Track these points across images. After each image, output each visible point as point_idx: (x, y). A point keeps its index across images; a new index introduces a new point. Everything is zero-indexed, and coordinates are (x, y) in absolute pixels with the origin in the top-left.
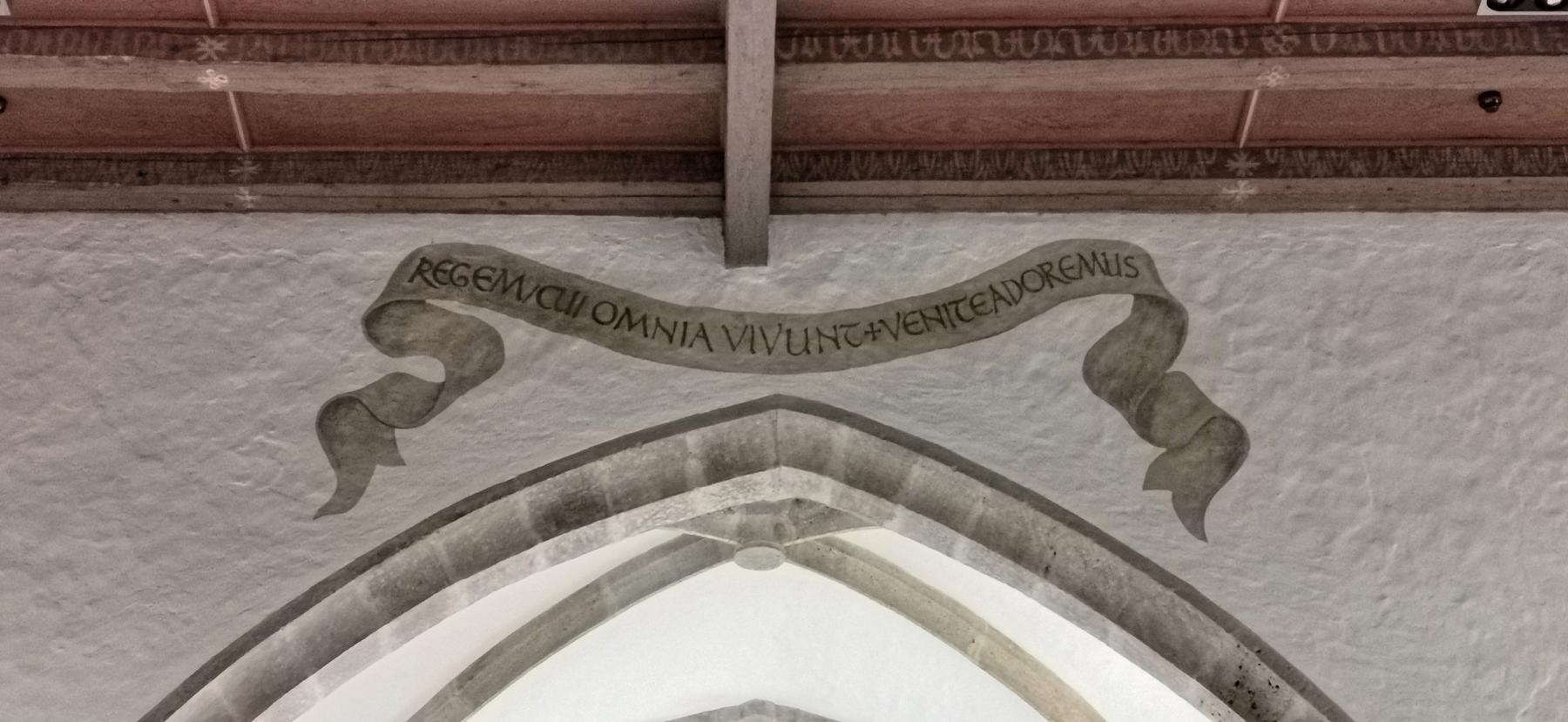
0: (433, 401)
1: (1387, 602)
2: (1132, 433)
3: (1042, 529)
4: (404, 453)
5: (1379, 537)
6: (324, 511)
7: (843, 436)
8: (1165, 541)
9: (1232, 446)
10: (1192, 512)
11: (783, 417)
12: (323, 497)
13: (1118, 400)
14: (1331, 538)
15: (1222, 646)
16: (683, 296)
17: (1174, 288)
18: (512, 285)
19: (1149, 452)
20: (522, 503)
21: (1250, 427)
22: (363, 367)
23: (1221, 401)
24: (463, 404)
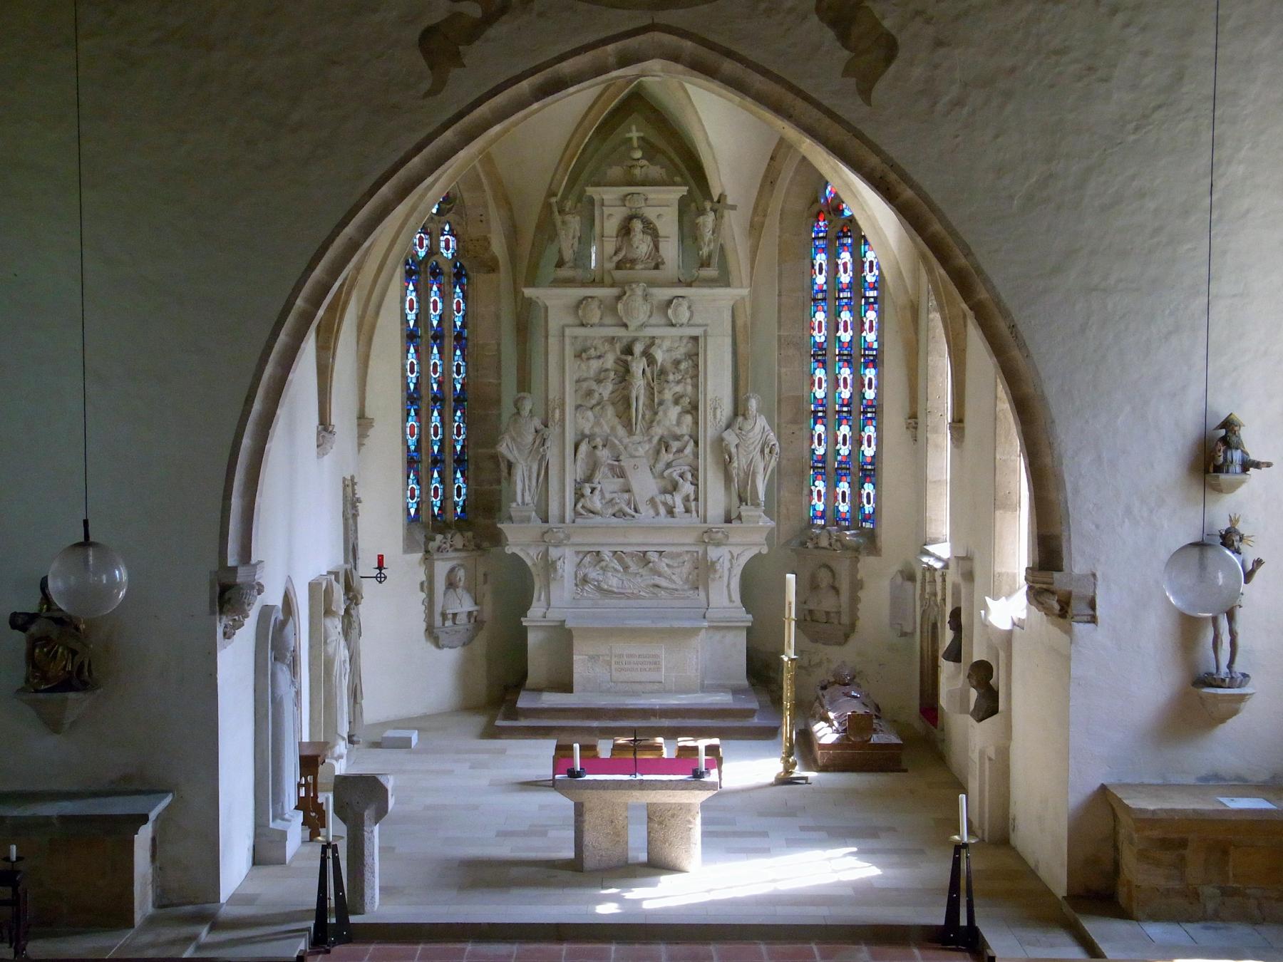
1: (959, 139)
2: (838, 44)
3: (789, 98)
4: (465, 61)
5: (958, 103)
6: (429, 94)
7: (688, 44)
8: (851, 108)
9: (890, 48)
10: (865, 92)
12: (426, 85)
13: (833, 24)
14: (935, 103)
15: (874, 161)
19: (846, 53)
20: (525, 85)
23: (887, 24)
24: (492, 32)
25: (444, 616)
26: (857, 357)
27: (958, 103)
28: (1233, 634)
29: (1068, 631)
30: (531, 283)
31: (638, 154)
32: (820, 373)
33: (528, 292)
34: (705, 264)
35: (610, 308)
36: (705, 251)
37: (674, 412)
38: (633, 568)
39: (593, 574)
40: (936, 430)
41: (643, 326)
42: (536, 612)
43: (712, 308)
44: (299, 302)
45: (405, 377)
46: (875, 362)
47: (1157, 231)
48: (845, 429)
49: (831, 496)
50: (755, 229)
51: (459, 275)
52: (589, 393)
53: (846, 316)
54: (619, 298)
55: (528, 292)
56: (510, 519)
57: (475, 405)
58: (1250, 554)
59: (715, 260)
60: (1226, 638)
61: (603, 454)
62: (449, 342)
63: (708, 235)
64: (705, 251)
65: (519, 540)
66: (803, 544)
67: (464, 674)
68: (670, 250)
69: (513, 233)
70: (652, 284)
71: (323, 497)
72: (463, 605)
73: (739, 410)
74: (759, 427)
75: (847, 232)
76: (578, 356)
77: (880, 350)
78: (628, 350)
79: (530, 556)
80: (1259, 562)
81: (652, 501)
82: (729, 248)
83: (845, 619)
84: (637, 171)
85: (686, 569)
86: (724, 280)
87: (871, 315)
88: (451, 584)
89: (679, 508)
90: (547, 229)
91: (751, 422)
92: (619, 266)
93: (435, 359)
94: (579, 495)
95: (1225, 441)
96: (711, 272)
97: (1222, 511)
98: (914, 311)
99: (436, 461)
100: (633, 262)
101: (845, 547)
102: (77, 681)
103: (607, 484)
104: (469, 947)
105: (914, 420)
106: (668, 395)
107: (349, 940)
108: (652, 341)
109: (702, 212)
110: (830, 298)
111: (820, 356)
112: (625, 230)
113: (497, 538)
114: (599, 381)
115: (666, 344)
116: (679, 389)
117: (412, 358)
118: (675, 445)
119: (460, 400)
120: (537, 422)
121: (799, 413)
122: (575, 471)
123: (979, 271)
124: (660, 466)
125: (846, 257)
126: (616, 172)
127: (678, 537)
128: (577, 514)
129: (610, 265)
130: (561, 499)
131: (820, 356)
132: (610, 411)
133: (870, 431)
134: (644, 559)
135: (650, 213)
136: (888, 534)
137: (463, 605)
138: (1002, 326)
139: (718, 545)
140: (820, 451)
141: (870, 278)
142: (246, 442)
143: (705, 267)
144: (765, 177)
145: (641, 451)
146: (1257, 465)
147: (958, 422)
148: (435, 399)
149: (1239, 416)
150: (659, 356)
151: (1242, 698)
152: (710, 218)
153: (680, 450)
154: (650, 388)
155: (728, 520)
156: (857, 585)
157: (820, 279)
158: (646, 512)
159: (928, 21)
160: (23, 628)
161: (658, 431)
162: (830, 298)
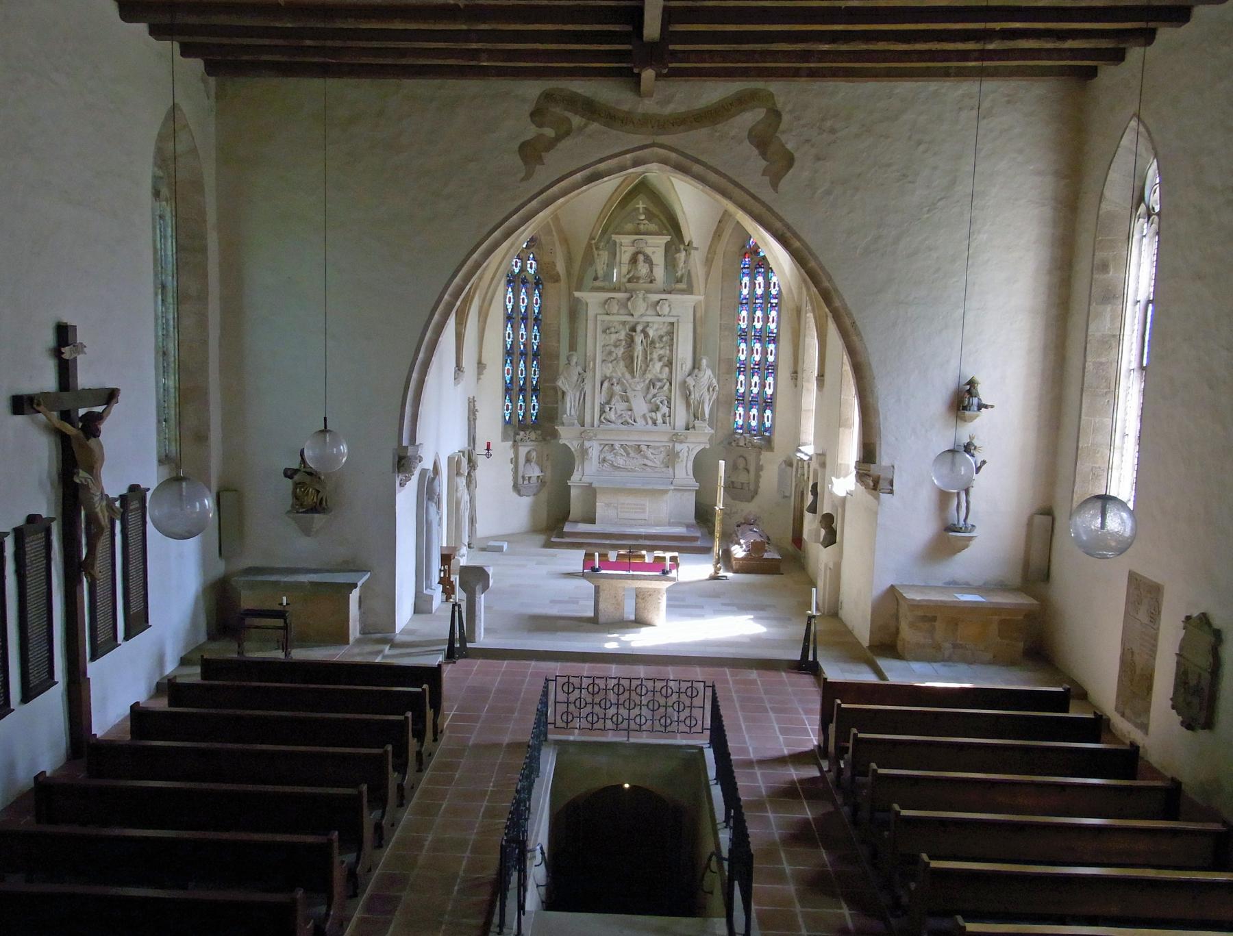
0: (551, 144)
3: (730, 187)
5: (828, 193)
6: (522, 180)
7: (673, 155)
8: (767, 194)
9: (790, 160)
10: (775, 185)
11: (656, 150)
12: (522, 175)
13: (758, 146)
15: (778, 225)
16: (625, 107)
17: (779, 106)
18: (573, 102)
19: (764, 163)
20: (578, 176)
21: (796, 155)
22: (532, 131)
23: (789, 146)
24: (560, 145)
25: (523, 478)
26: (765, 337)
27: (828, 193)
28: (968, 502)
29: (877, 498)
30: (579, 289)
31: (643, 217)
32: (743, 346)
33: (577, 294)
34: (679, 281)
35: (624, 304)
36: (679, 274)
37: (658, 365)
38: (632, 454)
39: (609, 457)
40: (808, 381)
41: (642, 315)
42: (575, 477)
43: (682, 306)
44: (446, 297)
45: (505, 341)
46: (775, 340)
47: (938, 270)
48: (756, 379)
49: (747, 417)
50: (709, 262)
51: (538, 283)
52: (610, 353)
53: (759, 313)
54: (629, 299)
55: (577, 294)
56: (563, 424)
57: (543, 356)
58: (980, 457)
59: (685, 279)
60: (964, 504)
61: (617, 388)
62: (531, 321)
63: (681, 265)
64: (679, 274)
65: (567, 436)
66: (730, 444)
67: (534, 511)
68: (659, 272)
69: (569, 260)
70: (648, 291)
71: (457, 408)
72: (535, 472)
73: (696, 365)
74: (707, 375)
75: (761, 265)
76: (604, 332)
77: (778, 334)
78: (633, 329)
79: (573, 446)
80: (984, 462)
81: (644, 416)
82: (693, 274)
83: (752, 487)
84: (642, 227)
85: (662, 456)
86: (689, 290)
87: (773, 314)
88: (528, 460)
89: (660, 421)
90: (589, 259)
91: (701, 375)
92: (629, 281)
93: (522, 331)
94: (602, 412)
95: (969, 391)
96: (682, 286)
97: (966, 432)
98: (799, 312)
99: (522, 390)
100: (638, 278)
101: (753, 446)
102: (318, 507)
103: (619, 405)
104: (533, 663)
105: (795, 374)
106: (655, 356)
107: (465, 657)
108: (647, 325)
109: (678, 251)
110: (750, 303)
111: (743, 336)
112: (634, 260)
113: (555, 435)
114: (616, 346)
115: (656, 326)
116: (661, 352)
117: (509, 330)
118: (658, 384)
119: (536, 355)
120: (579, 369)
121: (729, 368)
122: (600, 398)
123: (836, 290)
124: (650, 396)
125: (760, 279)
126: (629, 227)
127: (659, 437)
128: (601, 422)
129: (625, 280)
130: (592, 413)
131: (743, 336)
132: (622, 363)
133: (770, 380)
134: (638, 449)
135: (648, 251)
136: (777, 439)
137: (535, 472)
138: (848, 322)
139: (681, 442)
140: (742, 390)
141: (774, 292)
142: (415, 375)
143: (679, 282)
144: (715, 232)
145: (639, 388)
146: (986, 407)
147: (821, 376)
148: (522, 354)
149: (977, 378)
150: (651, 333)
151: (970, 538)
152: (683, 255)
153: (661, 388)
154: (645, 351)
155: (687, 429)
156: (759, 468)
157: (745, 292)
158: (641, 422)
159: (812, 146)
160: (291, 477)
161: (649, 376)
162: (750, 303)
